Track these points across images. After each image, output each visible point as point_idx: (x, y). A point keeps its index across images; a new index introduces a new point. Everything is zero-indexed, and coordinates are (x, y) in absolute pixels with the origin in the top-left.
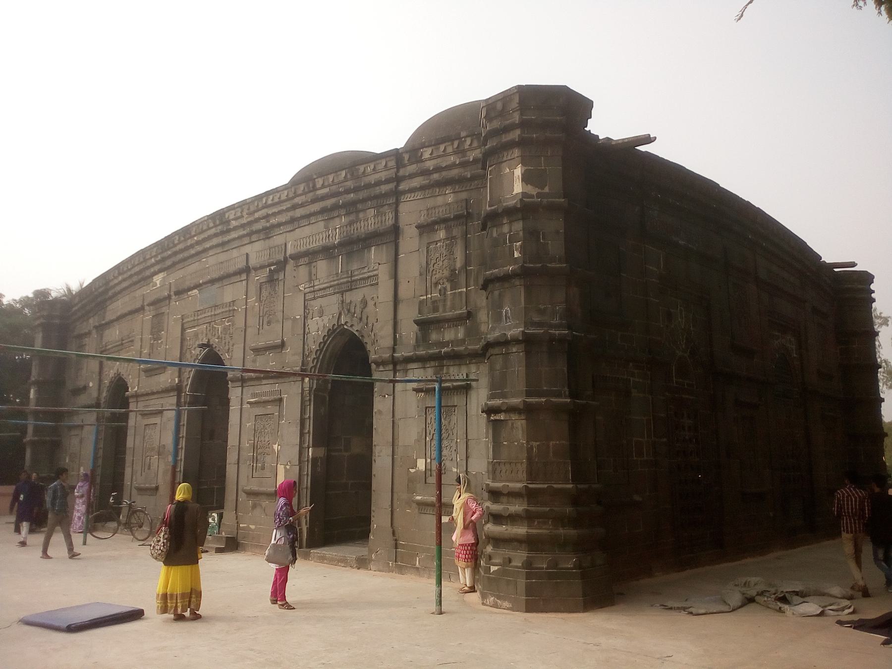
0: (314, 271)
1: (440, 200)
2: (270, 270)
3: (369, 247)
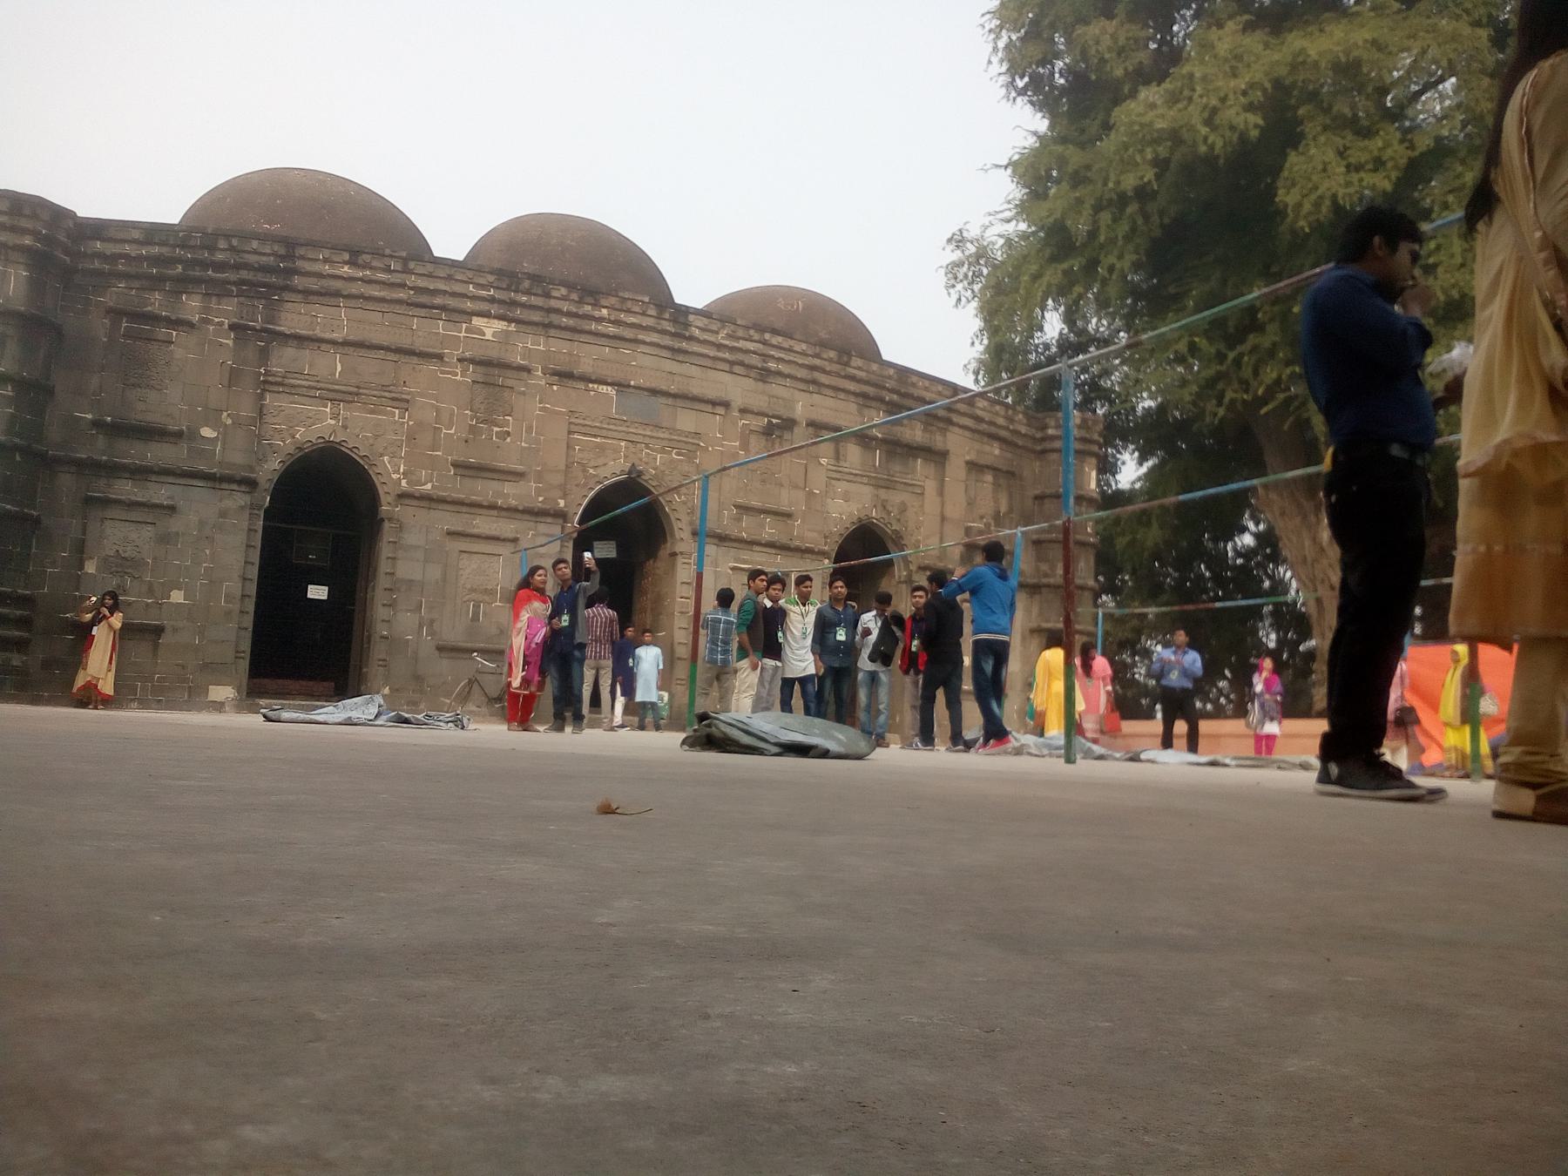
0: (842, 452)
1: (987, 448)
2: (770, 422)
3: (915, 457)
